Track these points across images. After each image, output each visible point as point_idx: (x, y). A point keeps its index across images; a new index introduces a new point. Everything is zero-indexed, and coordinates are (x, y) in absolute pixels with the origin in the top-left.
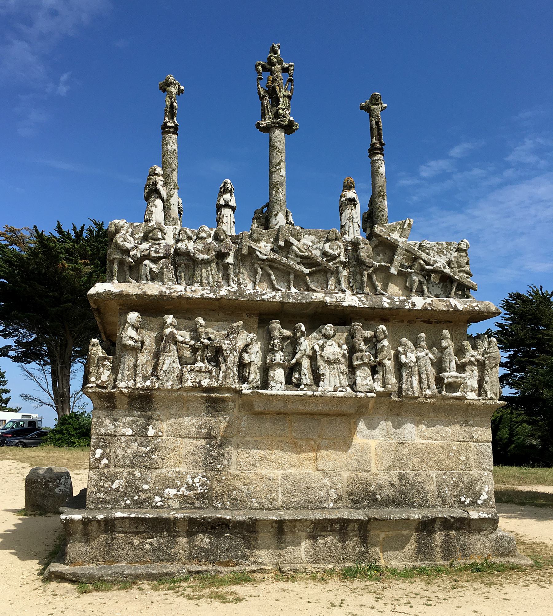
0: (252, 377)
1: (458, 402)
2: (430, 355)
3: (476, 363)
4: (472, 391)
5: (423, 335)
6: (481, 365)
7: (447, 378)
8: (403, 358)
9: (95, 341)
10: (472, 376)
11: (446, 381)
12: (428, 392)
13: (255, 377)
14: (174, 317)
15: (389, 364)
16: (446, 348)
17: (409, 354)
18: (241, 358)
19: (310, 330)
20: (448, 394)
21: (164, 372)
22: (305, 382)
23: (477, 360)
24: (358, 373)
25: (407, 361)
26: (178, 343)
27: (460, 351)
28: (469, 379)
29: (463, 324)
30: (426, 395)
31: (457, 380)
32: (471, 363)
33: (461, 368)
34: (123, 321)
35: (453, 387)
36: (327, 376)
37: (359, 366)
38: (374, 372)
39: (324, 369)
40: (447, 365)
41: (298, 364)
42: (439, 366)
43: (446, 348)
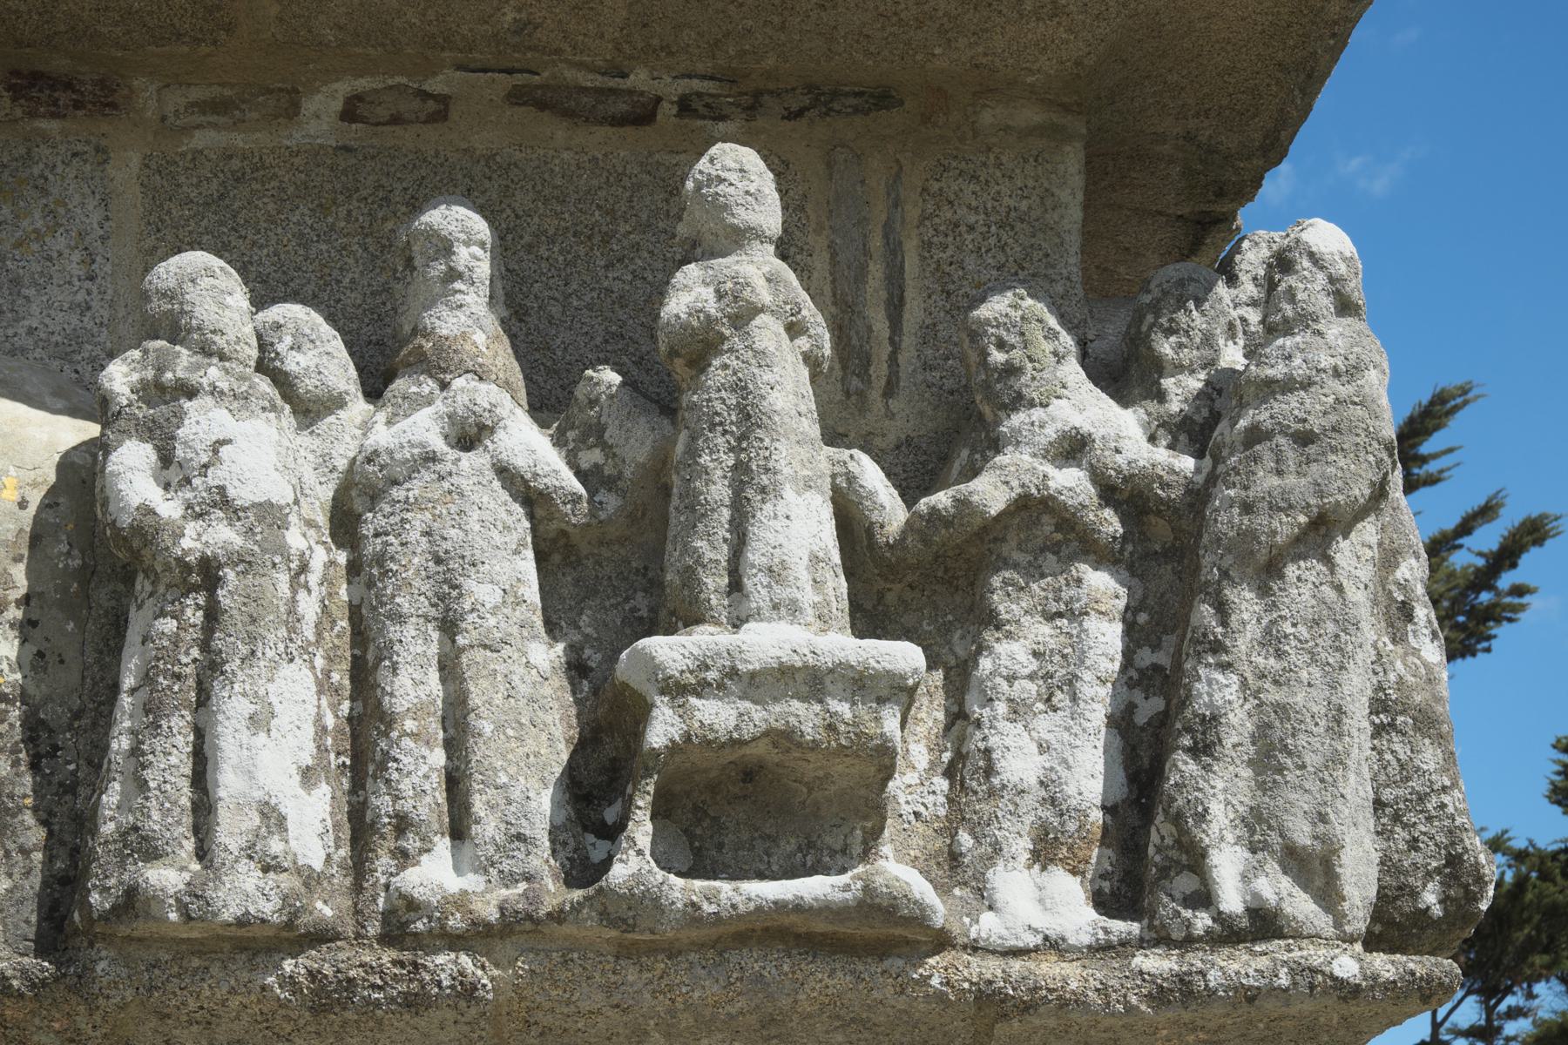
1: (827, 979)
2: (528, 443)
3: (1111, 523)
4: (1045, 852)
5: (461, 225)
6: (1171, 554)
7: (677, 690)
8: (134, 475)
10: (1057, 684)
11: (662, 729)
12: (435, 874)
16: (702, 345)
17: (202, 422)
20: (679, 889)
23: (1126, 493)
25: (169, 508)
27: (934, 412)
28: (1018, 710)
29: (1030, 115)
30: (412, 905)
31: (804, 716)
32: (1042, 530)
33: (922, 585)
35: (752, 803)
40: (712, 548)
42: (619, 568)
43: (702, 345)
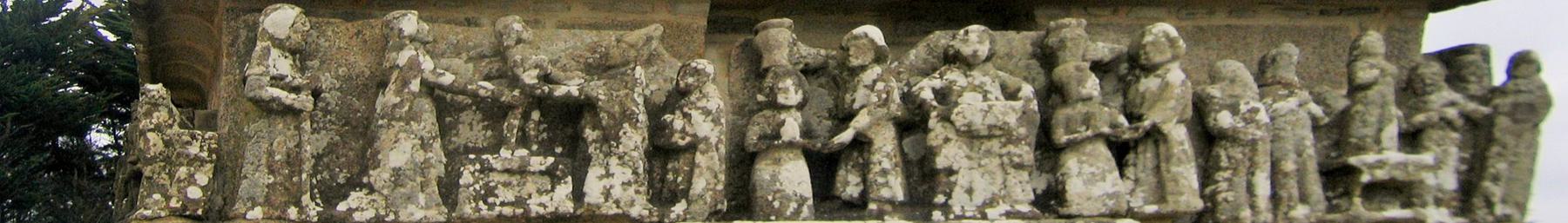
0: (699, 185)
9: (156, 89)
13: (707, 178)
14: (420, 18)
15: (1179, 134)
18: (657, 129)
19: (900, 38)
21: (397, 172)
22: (885, 193)
24: (1071, 162)
26: (437, 92)
34: (243, 33)
36: (962, 180)
37: (1073, 145)
38: (1121, 151)
39: (950, 154)
41: (861, 143)
